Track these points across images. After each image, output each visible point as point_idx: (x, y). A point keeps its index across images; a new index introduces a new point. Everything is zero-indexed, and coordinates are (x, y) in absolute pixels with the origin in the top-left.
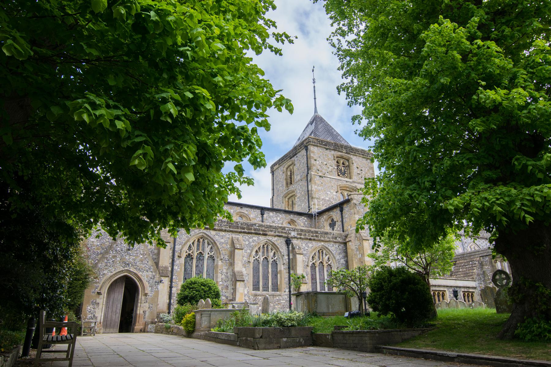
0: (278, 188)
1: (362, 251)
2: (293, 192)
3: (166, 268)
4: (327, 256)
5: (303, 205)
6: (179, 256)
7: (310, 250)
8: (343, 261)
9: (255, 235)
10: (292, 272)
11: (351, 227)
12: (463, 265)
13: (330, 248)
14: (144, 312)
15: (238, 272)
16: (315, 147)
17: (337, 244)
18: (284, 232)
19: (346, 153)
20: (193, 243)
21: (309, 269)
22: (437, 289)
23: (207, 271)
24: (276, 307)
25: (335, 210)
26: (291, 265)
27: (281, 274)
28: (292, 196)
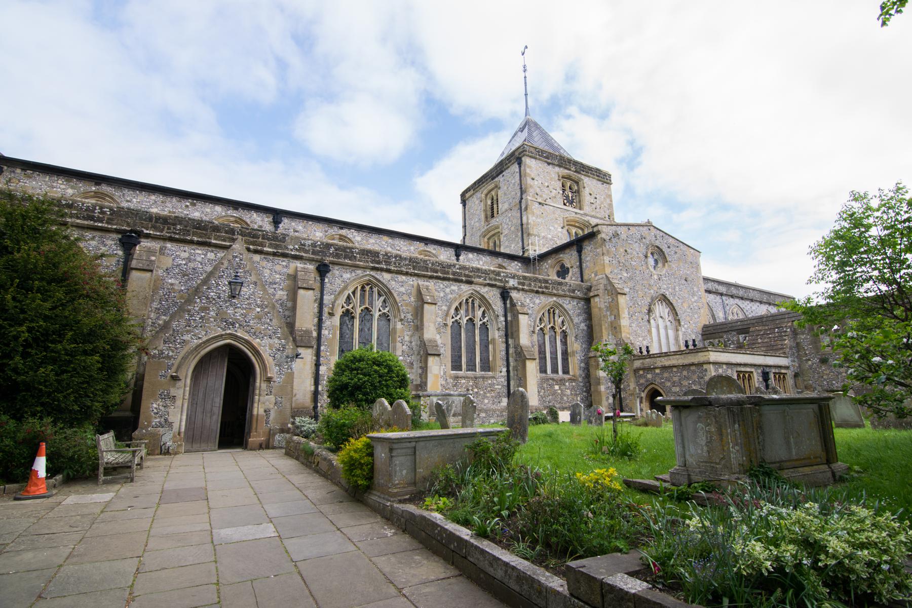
0: (472, 224)
1: (616, 311)
2: (497, 227)
3: (308, 332)
4: (561, 319)
5: (513, 246)
6: (329, 313)
7: (536, 308)
8: (583, 326)
9: (454, 283)
10: (510, 341)
11: (596, 275)
12: (762, 333)
13: (565, 305)
14: (265, 411)
15: (430, 341)
16: (532, 160)
17: (575, 300)
18: (499, 280)
19: (575, 172)
20: (354, 293)
21: (535, 337)
22: (743, 369)
23: (378, 338)
24: (488, 395)
25: (567, 251)
26: (510, 331)
27: (494, 344)
28: (493, 235)
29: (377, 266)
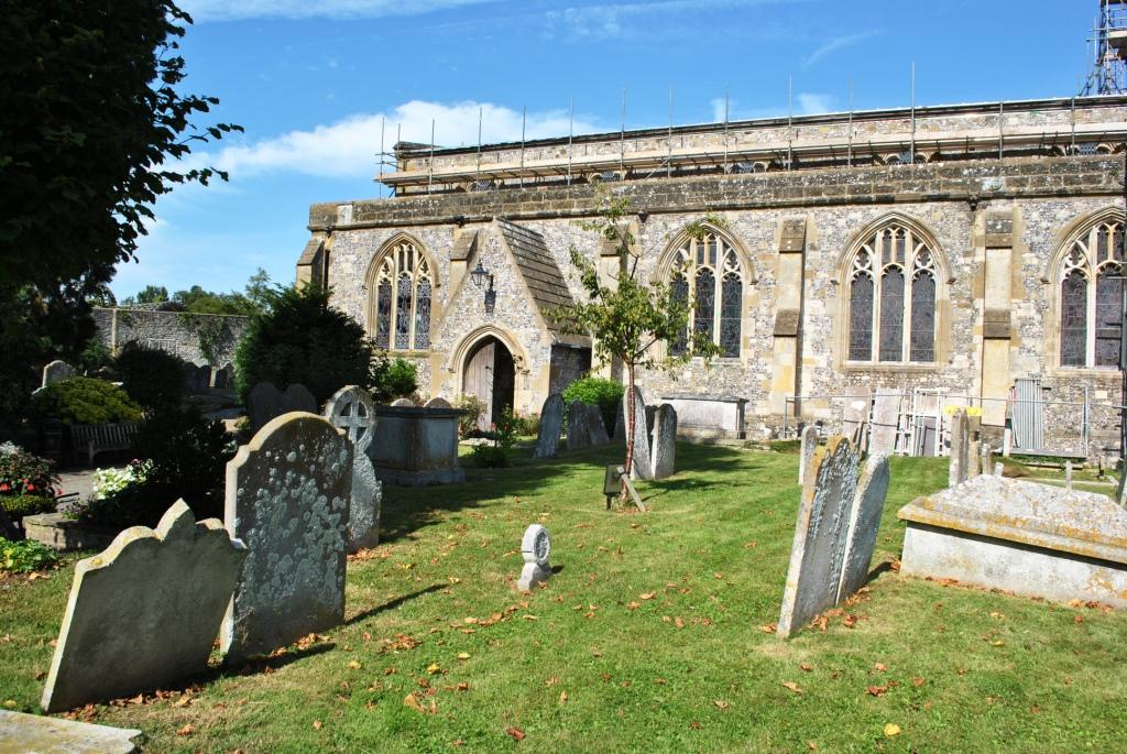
9: (854, 207)
18: (957, 184)
29: (714, 203)
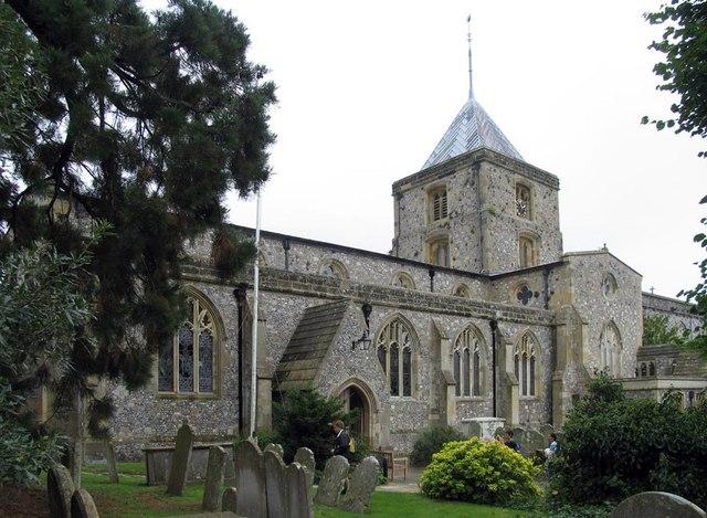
26: (496, 360)
